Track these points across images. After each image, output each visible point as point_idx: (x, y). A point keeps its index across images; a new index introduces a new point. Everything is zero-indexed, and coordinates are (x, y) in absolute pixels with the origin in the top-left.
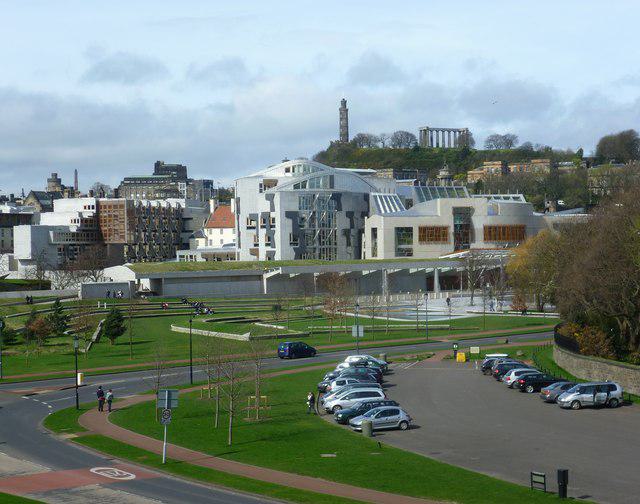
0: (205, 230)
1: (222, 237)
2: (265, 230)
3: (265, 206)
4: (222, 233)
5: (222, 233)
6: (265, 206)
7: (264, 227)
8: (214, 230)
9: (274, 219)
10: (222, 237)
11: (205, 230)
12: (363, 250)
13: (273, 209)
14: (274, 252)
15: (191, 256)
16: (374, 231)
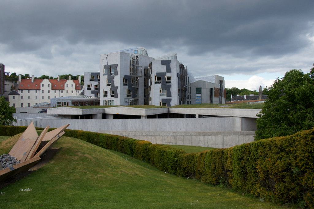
0: (18, 91)
1: (29, 94)
2: (160, 85)
3: (163, 69)
4: (29, 92)
5: (29, 92)
6: (163, 69)
7: (156, 83)
8: (23, 90)
9: (169, 78)
10: (29, 94)
11: (18, 91)
12: (187, 100)
13: (169, 70)
14: (171, 100)
15: (65, 103)
16: (199, 90)
